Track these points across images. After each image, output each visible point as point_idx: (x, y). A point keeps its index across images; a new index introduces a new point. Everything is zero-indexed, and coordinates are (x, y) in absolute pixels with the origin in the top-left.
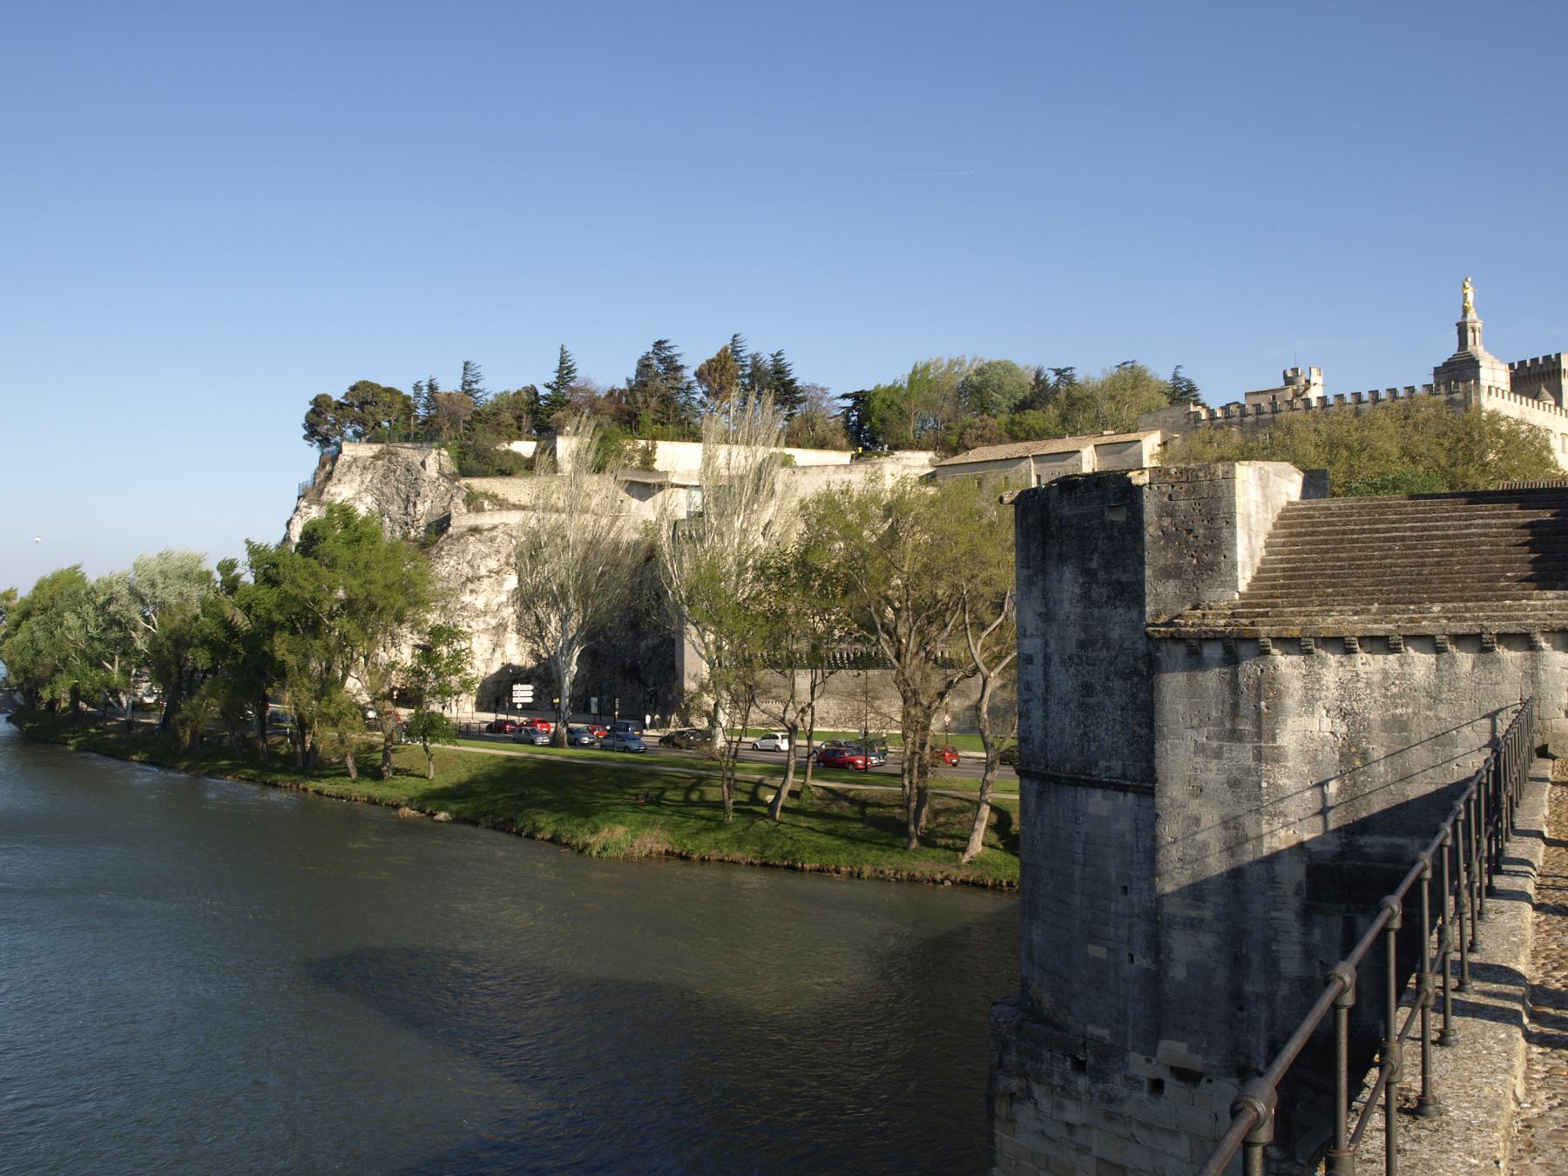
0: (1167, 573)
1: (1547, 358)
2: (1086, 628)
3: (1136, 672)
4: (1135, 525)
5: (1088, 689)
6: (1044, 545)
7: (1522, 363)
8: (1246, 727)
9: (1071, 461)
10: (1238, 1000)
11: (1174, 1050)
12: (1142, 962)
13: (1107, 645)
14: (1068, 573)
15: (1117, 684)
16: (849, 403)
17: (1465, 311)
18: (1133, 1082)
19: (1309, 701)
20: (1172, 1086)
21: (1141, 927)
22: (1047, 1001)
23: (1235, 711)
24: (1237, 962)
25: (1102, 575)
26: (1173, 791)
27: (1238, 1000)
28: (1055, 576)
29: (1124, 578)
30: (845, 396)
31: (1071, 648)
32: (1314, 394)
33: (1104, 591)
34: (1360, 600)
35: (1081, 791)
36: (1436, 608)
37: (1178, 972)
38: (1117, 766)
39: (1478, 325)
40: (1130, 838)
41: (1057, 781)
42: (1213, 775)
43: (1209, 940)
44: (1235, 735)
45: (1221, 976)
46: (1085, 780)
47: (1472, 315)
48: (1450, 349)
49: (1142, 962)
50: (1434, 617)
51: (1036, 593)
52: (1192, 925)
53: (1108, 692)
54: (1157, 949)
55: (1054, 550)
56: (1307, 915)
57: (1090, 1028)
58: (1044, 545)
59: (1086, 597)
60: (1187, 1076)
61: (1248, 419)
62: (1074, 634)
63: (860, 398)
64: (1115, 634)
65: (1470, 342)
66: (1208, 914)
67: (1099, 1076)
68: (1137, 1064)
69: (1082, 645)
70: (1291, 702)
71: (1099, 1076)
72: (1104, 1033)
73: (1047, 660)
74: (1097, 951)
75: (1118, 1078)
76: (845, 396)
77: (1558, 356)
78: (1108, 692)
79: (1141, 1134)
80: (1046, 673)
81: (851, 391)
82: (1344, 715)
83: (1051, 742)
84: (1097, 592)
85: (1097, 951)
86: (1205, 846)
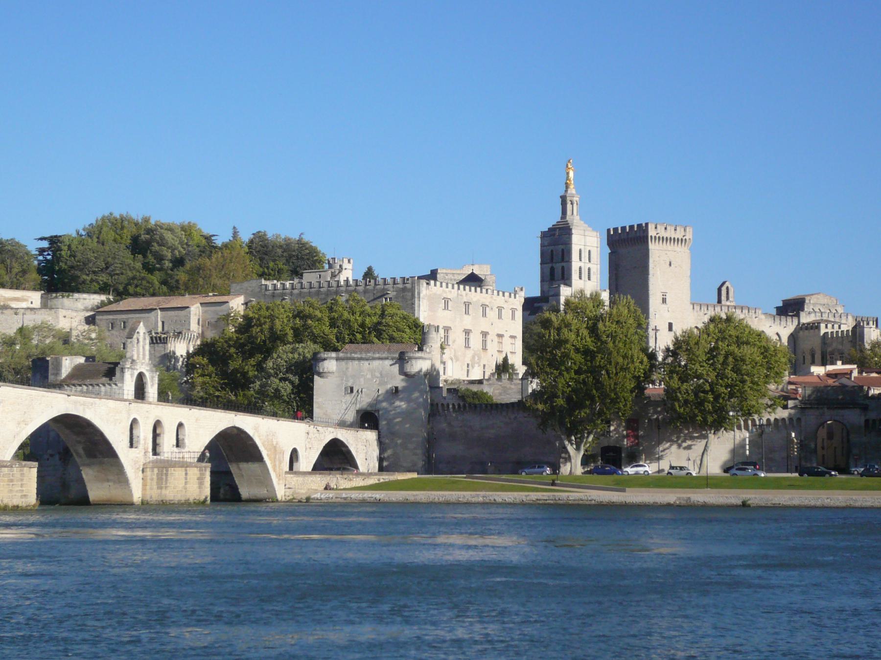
0: (53, 374)
1: (639, 226)
4: (48, 367)
7: (616, 230)
9: (182, 313)
11: (50, 452)
16: (45, 244)
17: (567, 186)
30: (41, 239)
32: (342, 278)
34: (77, 379)
39: (576, 199)
47: (572, 190)
48: (552, 219)
50: (88, 381)
60: (52, 455)
61: (295, 291)
63: (54, 241)
65: (569, 212)
76: (41, 239)
77: (647, 224)
81: (47, 235)
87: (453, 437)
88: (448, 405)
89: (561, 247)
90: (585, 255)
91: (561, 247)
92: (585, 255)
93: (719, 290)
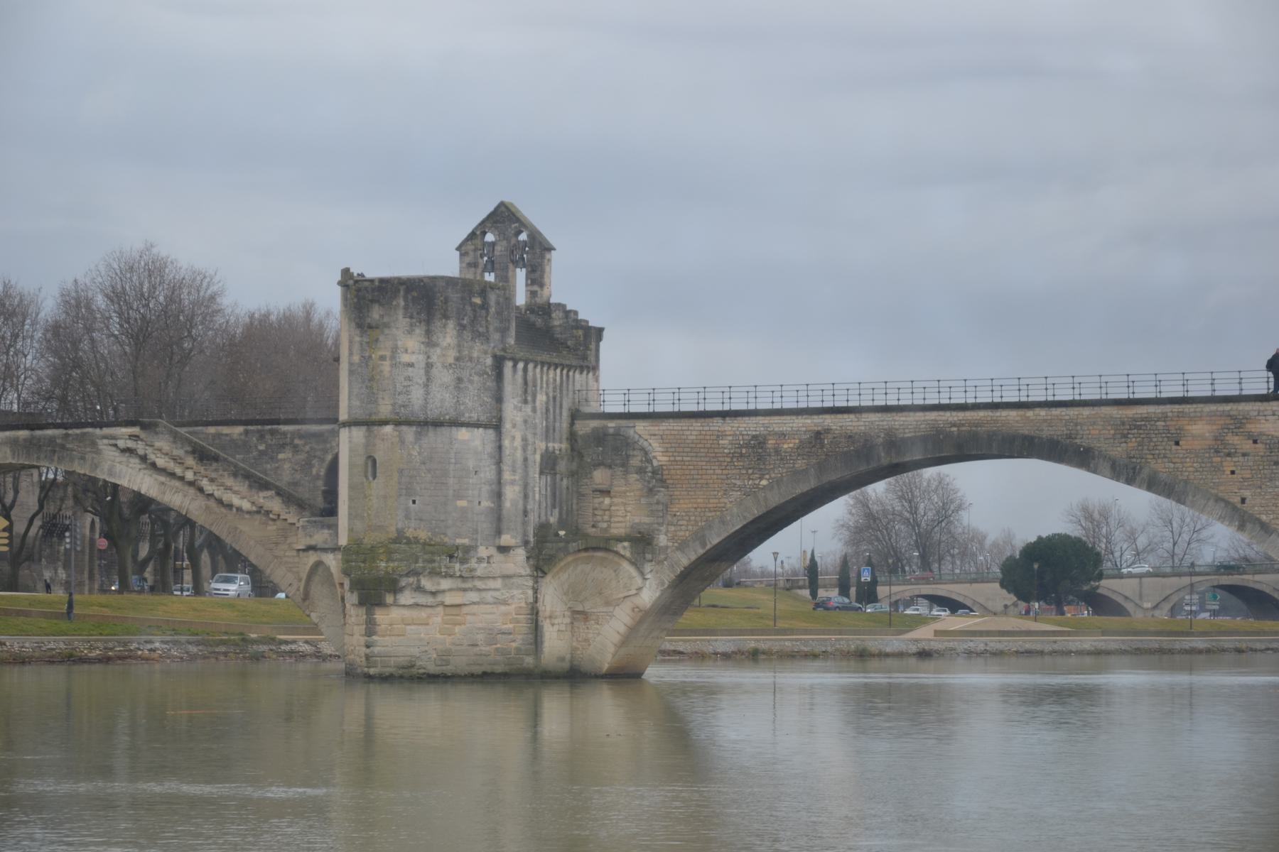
5: (460, 380)
10: (525, 513)
11: (506, 539)
12: (487, 504)
13: (471, 359)
15: (476, 378)
18: (480, 560)
20: (498, 557)
21: (486, 488)
22: (423, 535)
23: (526, 392)
24: (526, 497)
26: (507, 426)
27: (525, 513)
28: (438, 324)
31: (451, 360)
35: (454, 429)
37: (507, 504)
40: (480, 448)
41: (437, 424)
42: (519, 419)
43: (517, 488)
44: (525, 402)
45: (521, 503)
46: (456, 423)
49: (487, 504)
52: (513, 483)
53: (471, 382)
54: (498, 496)
56: (541, 473)
57: (459, 541)
60: (503, 550)
62: (452, 354)
64: (475, 355)
66: (517, 478)
67: (464, 561)
68: (483, 552)
69: (457, 359)
71: (464, 561)
72: (466, 541)
73: (429, 366)
74: (462, 503)
75: (474, 560)
78: (471, 382)
79: (479, 584)
83: (430, 406)
85: (462, 503)
86: (516, 449)
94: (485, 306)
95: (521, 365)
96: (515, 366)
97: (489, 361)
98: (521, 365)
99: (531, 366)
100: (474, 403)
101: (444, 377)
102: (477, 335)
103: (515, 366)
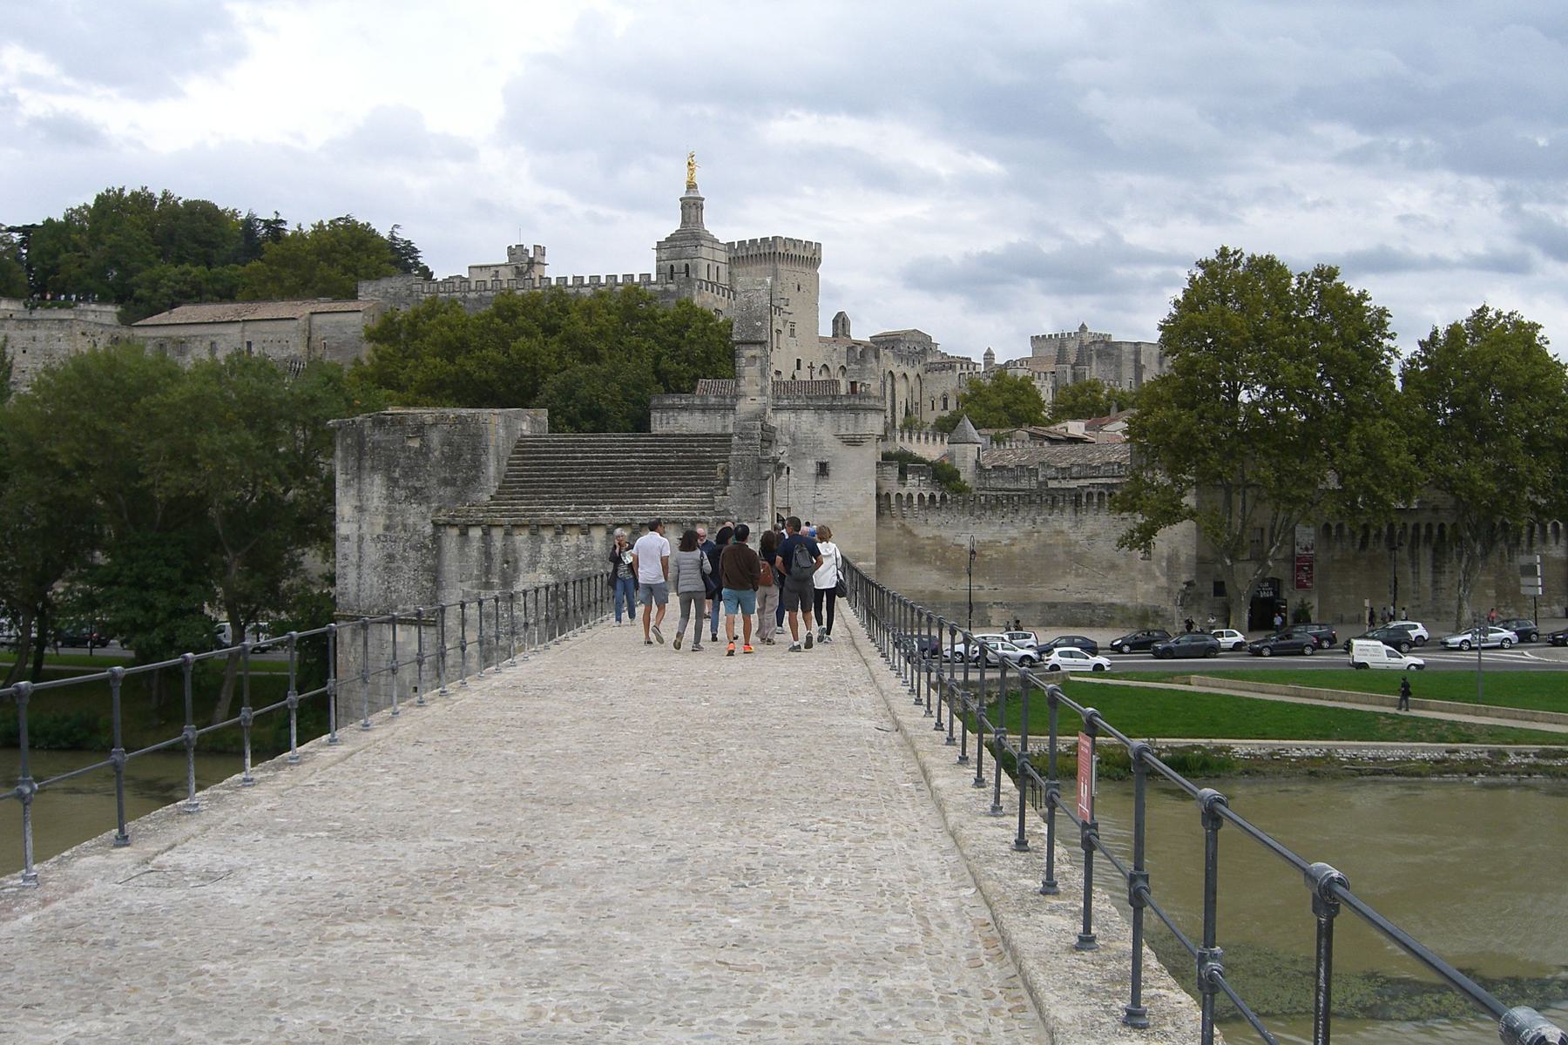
2: (390, 517)
3: (426, 546)
5: (391, 557)
6: (360, 459)
8: (496, 580)
13: (405, 526)
14: (378, 479)
15: (412, 554)
19: (533, 564)
25: (402, 481)
29: (418, 484)
31: (379, 530)
33: (403, 493)
36: (608, 507)
38: (411, 608)
44: (488, 585)
51: (353, 492)
55: (368, 464)
58: (360, 459)
59: (390, 497)
64: (410, 521)
69: (387, 528)
70: (522, 565)
73: (361, 538)
80: (359, 547)
82: (552, 571)
83: (362, 594)
84: (400, 493)
87: (916, 555)
88: (910, 496)
89: (684, 262)
90: (713, 271)
91: (684, 262)
92: (713, 271)
93: (835, 322)
94: (424, 451)
95: (475, 533)
96: (464, 534)
97: (429, 529)
98: (475, 533)
99: (497, 534)
100: (408, 594)
101: (373, 553)
102: (417, 494)
103: (464, 534)
